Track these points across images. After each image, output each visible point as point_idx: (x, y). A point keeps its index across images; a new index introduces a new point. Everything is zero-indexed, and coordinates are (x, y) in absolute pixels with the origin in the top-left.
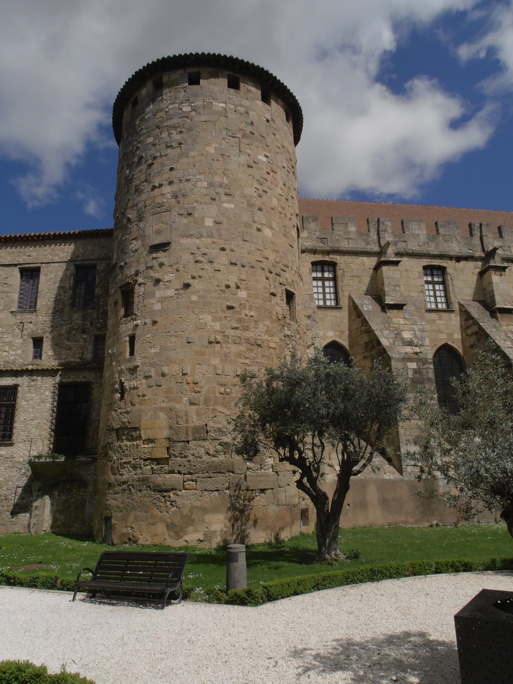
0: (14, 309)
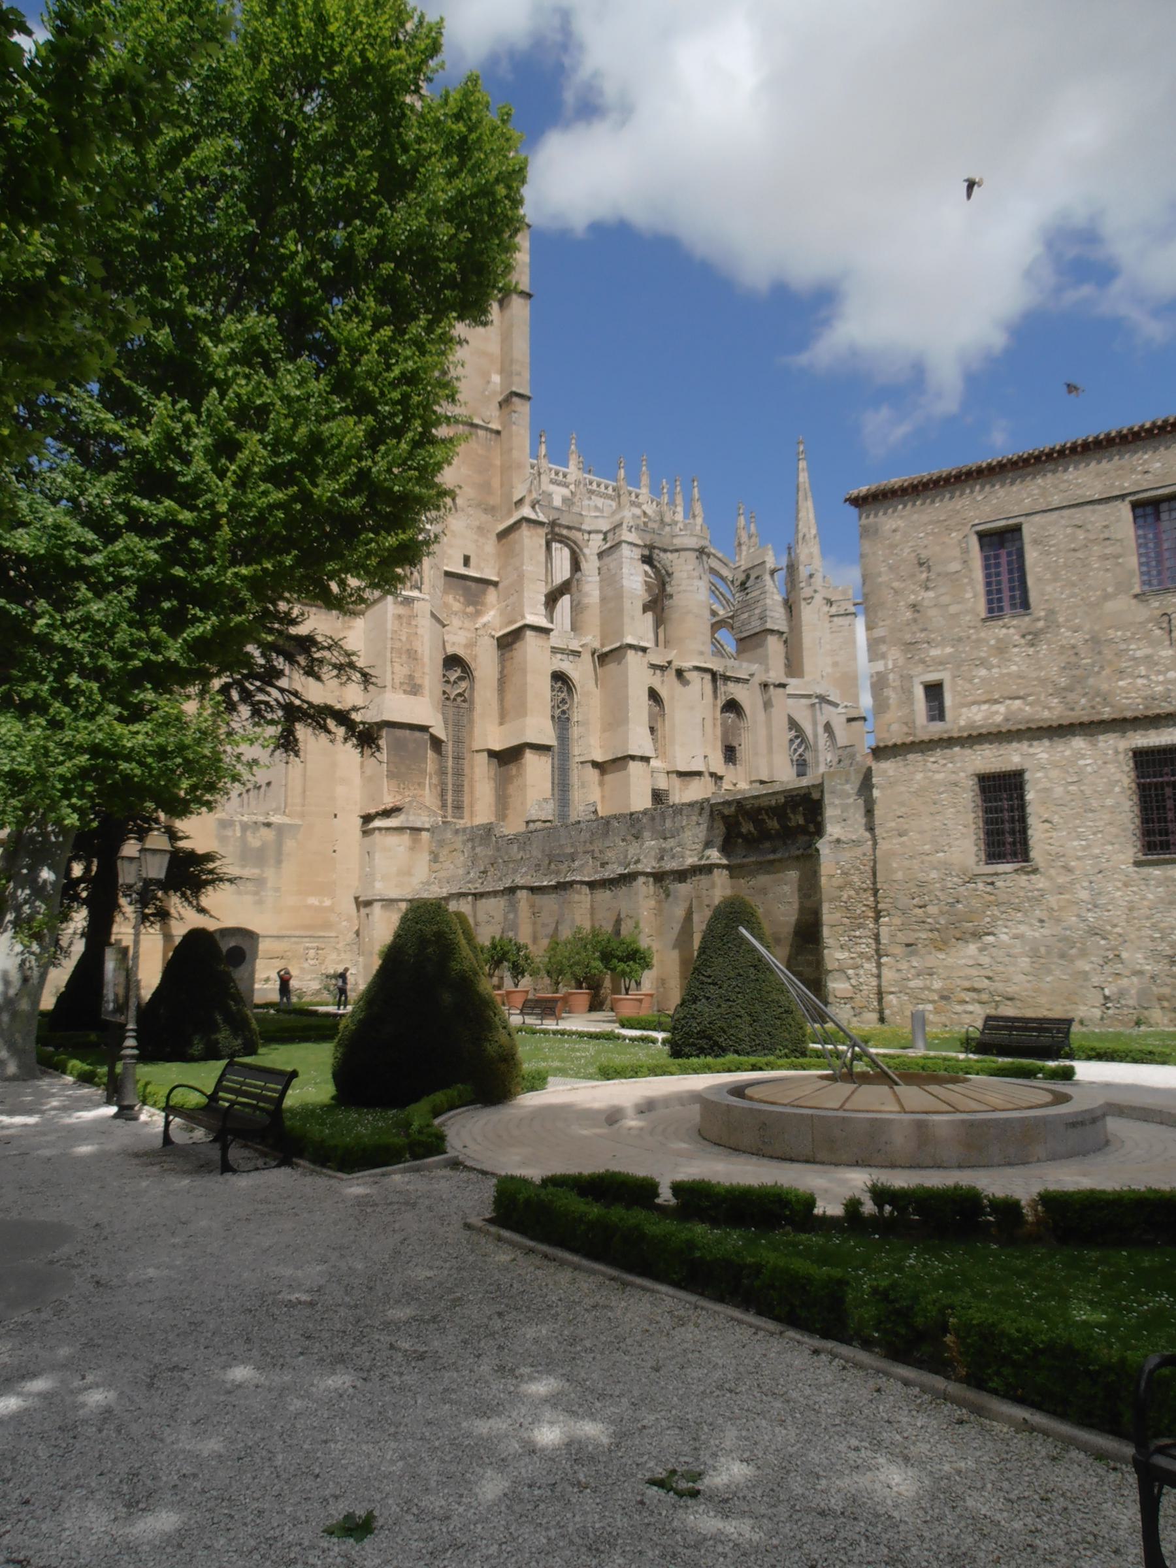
0: (1137, 589)
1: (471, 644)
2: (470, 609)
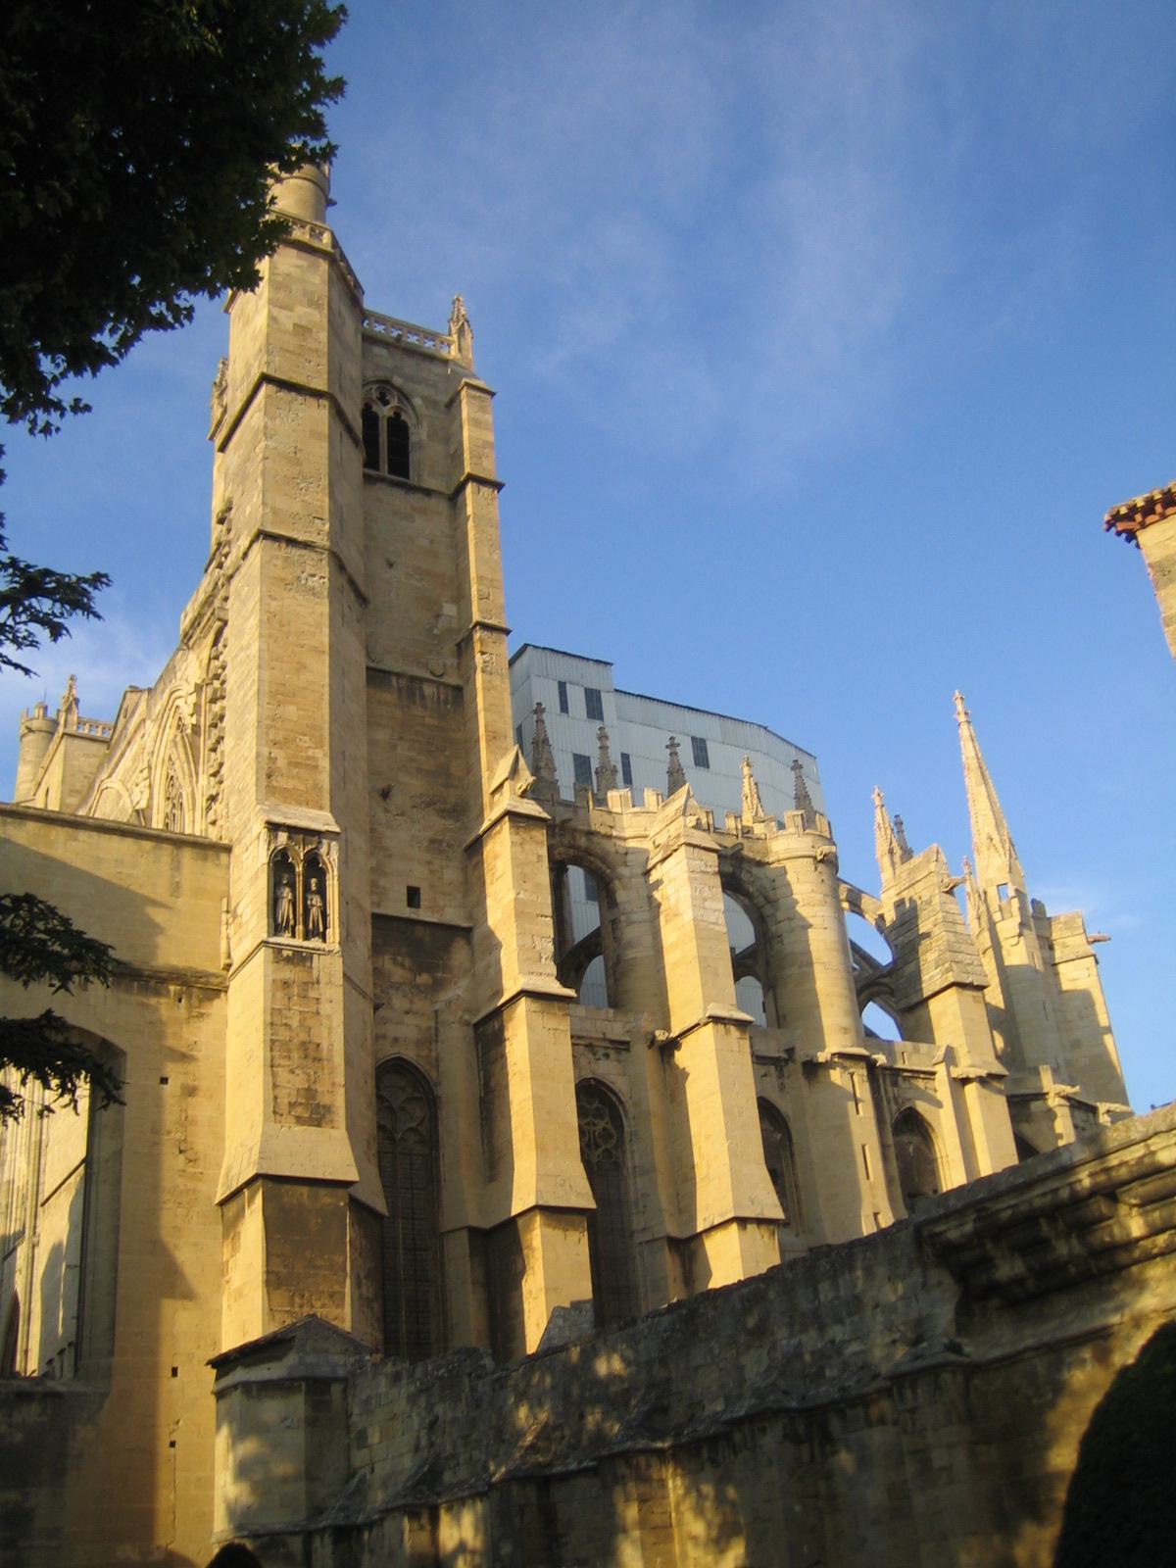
1: (431, 1038)
2: (424, 978)
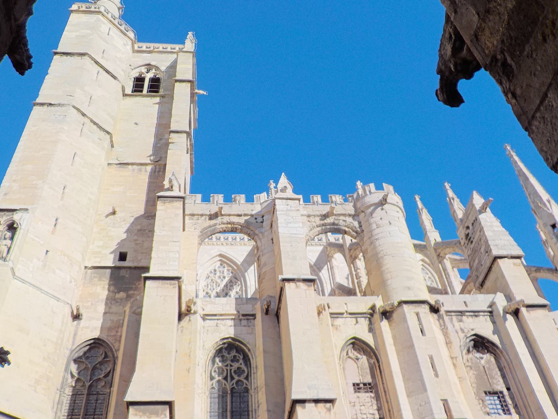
2: (122, 295)
